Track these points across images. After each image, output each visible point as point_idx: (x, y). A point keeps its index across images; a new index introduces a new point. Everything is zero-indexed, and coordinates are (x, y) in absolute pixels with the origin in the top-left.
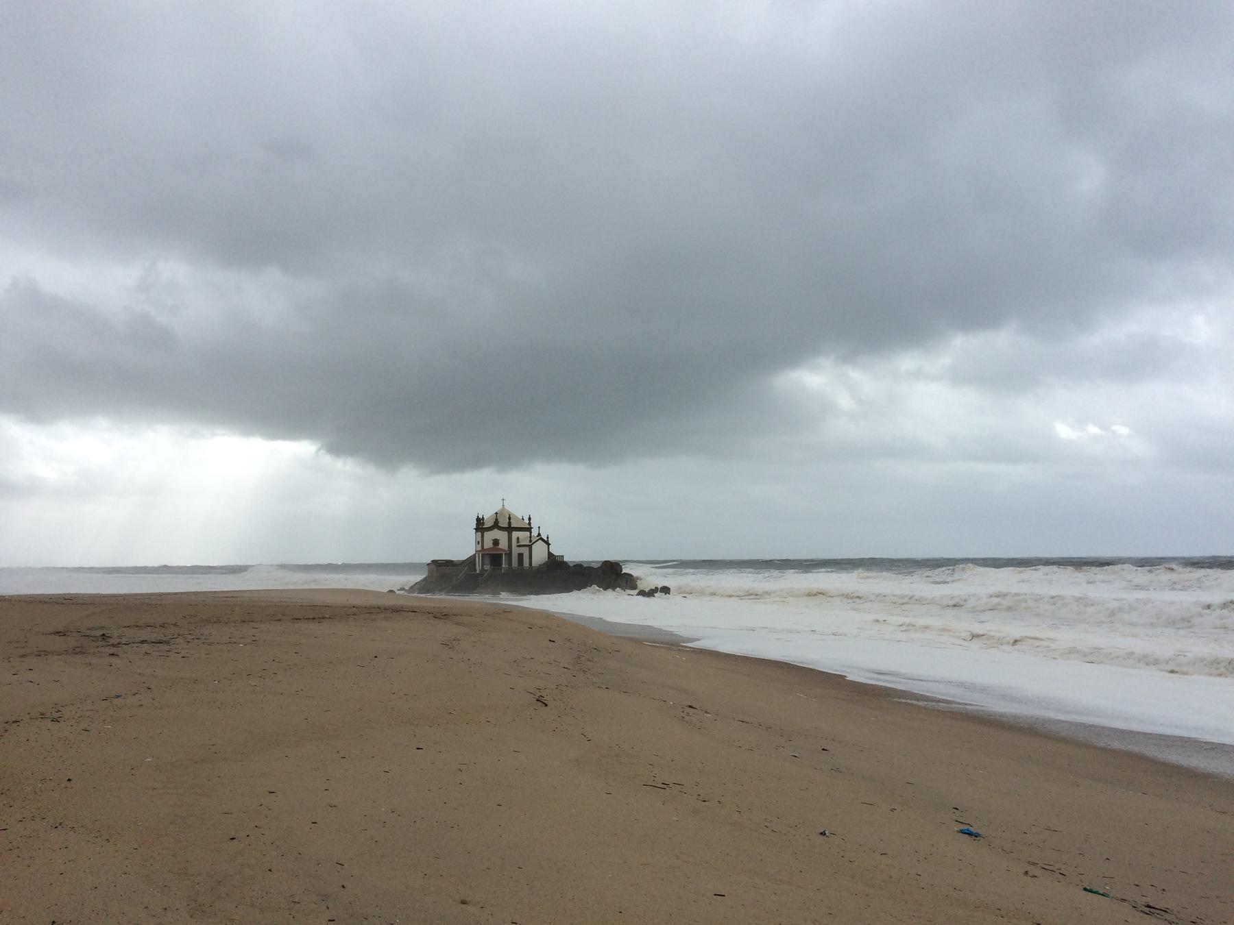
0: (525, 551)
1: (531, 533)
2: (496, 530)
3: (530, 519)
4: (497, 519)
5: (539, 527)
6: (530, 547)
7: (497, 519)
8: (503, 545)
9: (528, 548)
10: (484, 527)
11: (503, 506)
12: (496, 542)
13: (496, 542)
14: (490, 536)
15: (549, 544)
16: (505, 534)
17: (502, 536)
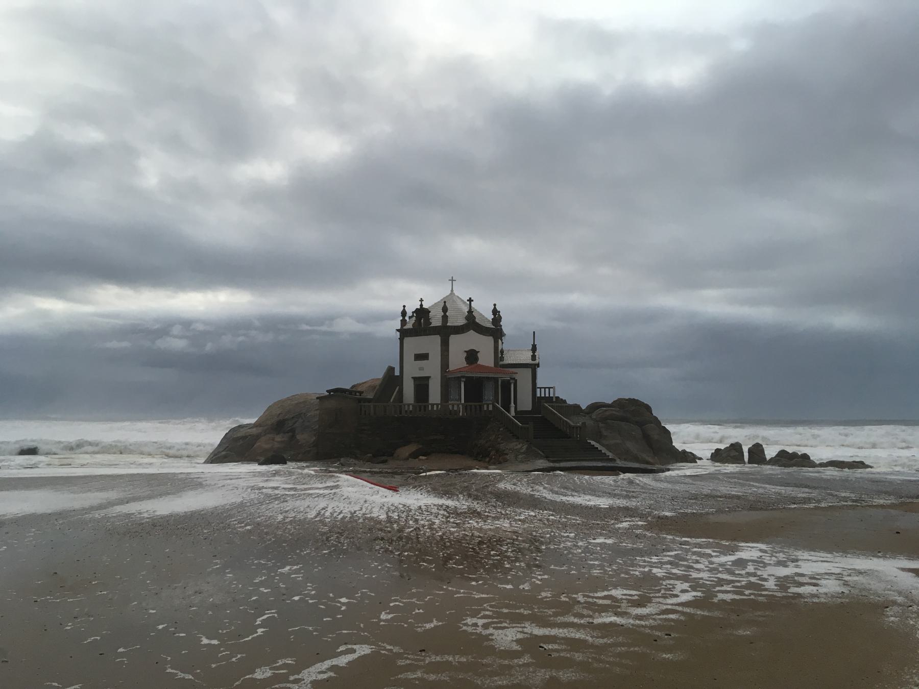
0: (523, 377)
1: (503, 343)
2: (472, 332)
3: (500, 318)
4: (470, 312)
5: (534, 332)
6: (533, 367)
7: (470, 312)
8: (486, 359)
9: (530, 370)
10: (448, 324)
11: (452, 290)
12: (472, 356)
13: (472, 356)
14: (459, 345)
15: (538, 367)
16: (490, 340)
17: (484, 346)
